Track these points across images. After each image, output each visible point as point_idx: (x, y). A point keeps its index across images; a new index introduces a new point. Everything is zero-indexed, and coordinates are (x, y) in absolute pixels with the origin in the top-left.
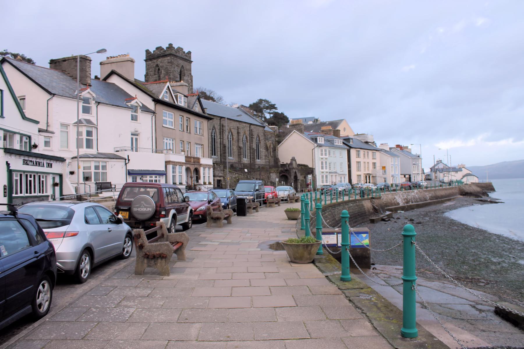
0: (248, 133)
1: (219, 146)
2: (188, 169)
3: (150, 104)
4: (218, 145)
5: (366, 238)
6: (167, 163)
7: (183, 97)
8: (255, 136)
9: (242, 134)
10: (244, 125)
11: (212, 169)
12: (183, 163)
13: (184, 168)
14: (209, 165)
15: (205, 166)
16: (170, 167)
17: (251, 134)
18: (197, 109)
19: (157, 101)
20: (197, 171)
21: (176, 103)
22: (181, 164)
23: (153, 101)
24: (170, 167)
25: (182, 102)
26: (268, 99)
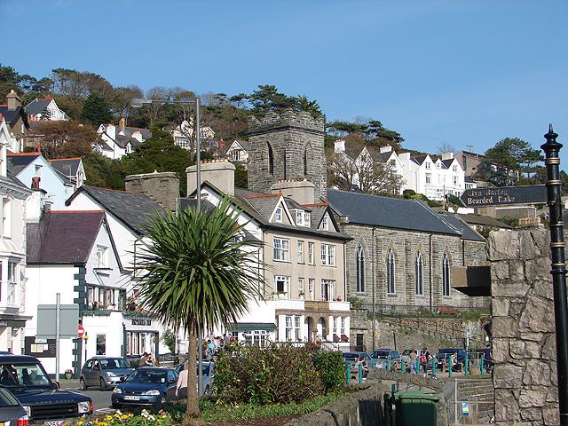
0: (425, 249)
1: (370, 274)
2: (309, 321)
3: (258, 233)
4: (368, 274)
5: (465, 406)
6: (278, 312)
7: (303, 213)
8: (441, 254)
9: (414, 251)
10: (419, 234)
11: (347, 320)
12: (301, 311)
13: (302, 319)
14: (343, 312)
15: (336, 314)
16: (282, 318)
17: (433, 251)
18: (328, 227)
19: (266, 228)
20: (324, 322)
21: (293, 224)
22: (298, 313)
23: (260, 227)
24: (282, 318)
25: (304, 222)
26: (522, 138)
